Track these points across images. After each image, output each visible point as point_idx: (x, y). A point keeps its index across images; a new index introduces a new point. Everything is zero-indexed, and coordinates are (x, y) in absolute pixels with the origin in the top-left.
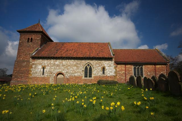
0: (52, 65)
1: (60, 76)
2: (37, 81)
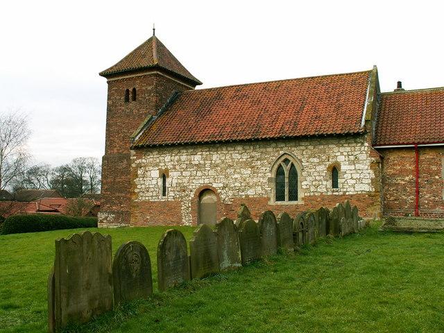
0: (184, 166)
1: (207, 198)
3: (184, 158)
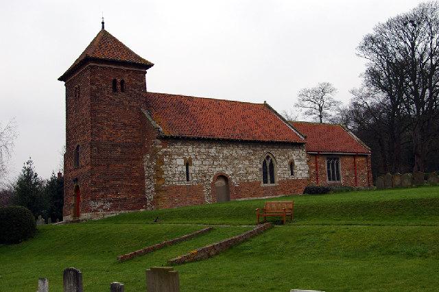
1: (221, 183)
2: (179, 196)
3: (203, 150)
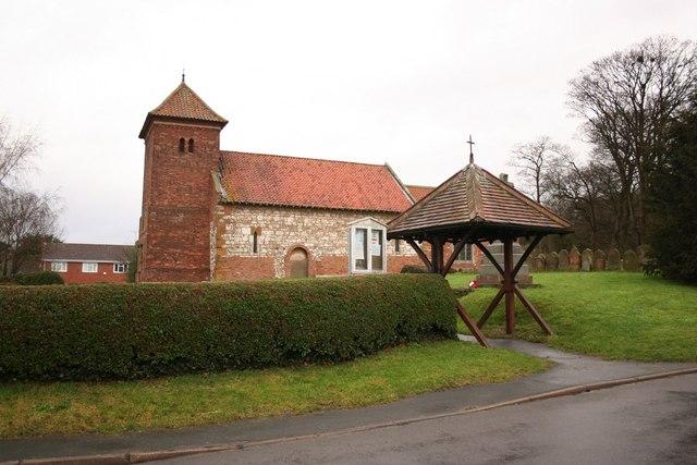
1: (299, 256)
3: (277, 218)
